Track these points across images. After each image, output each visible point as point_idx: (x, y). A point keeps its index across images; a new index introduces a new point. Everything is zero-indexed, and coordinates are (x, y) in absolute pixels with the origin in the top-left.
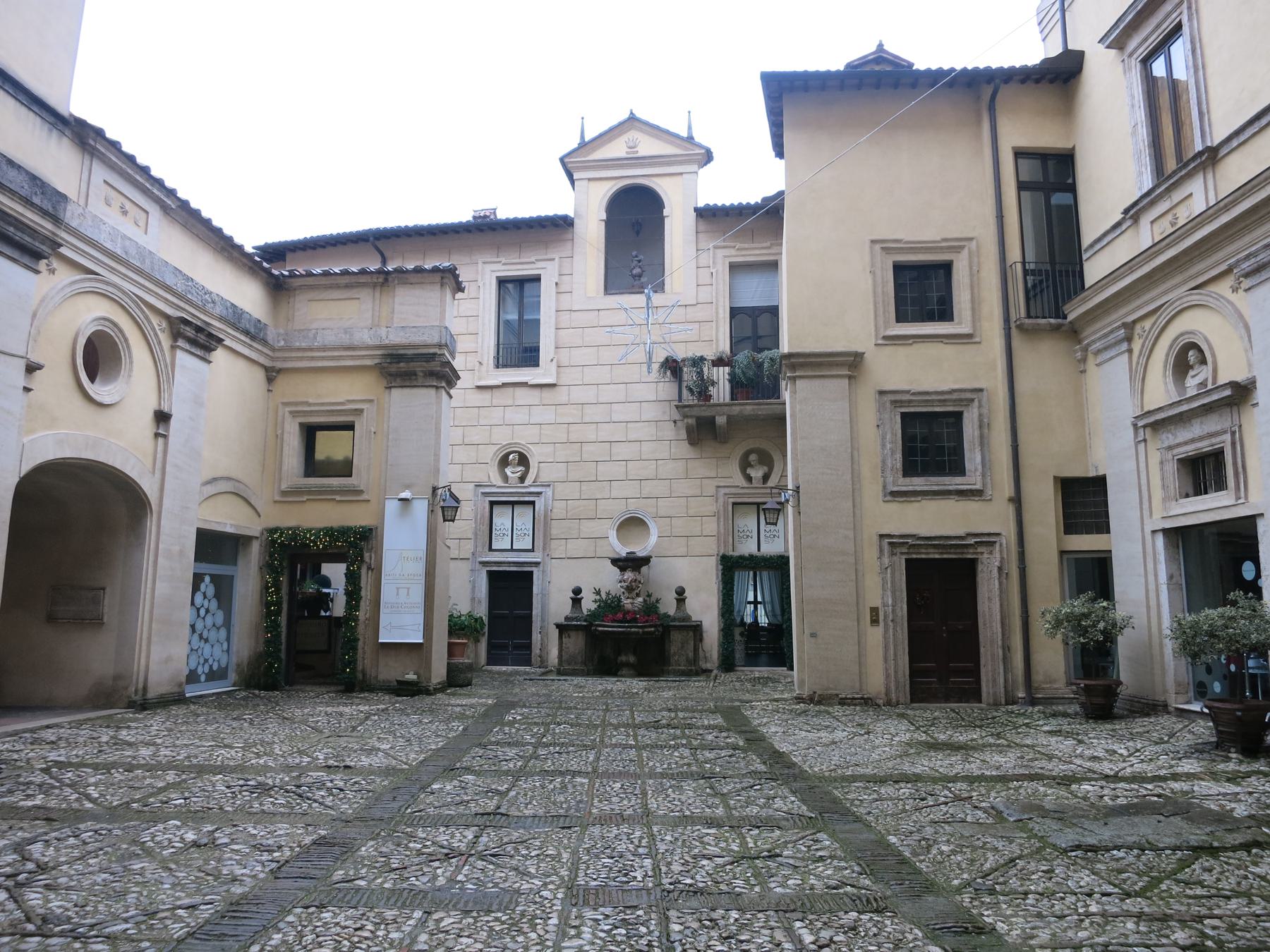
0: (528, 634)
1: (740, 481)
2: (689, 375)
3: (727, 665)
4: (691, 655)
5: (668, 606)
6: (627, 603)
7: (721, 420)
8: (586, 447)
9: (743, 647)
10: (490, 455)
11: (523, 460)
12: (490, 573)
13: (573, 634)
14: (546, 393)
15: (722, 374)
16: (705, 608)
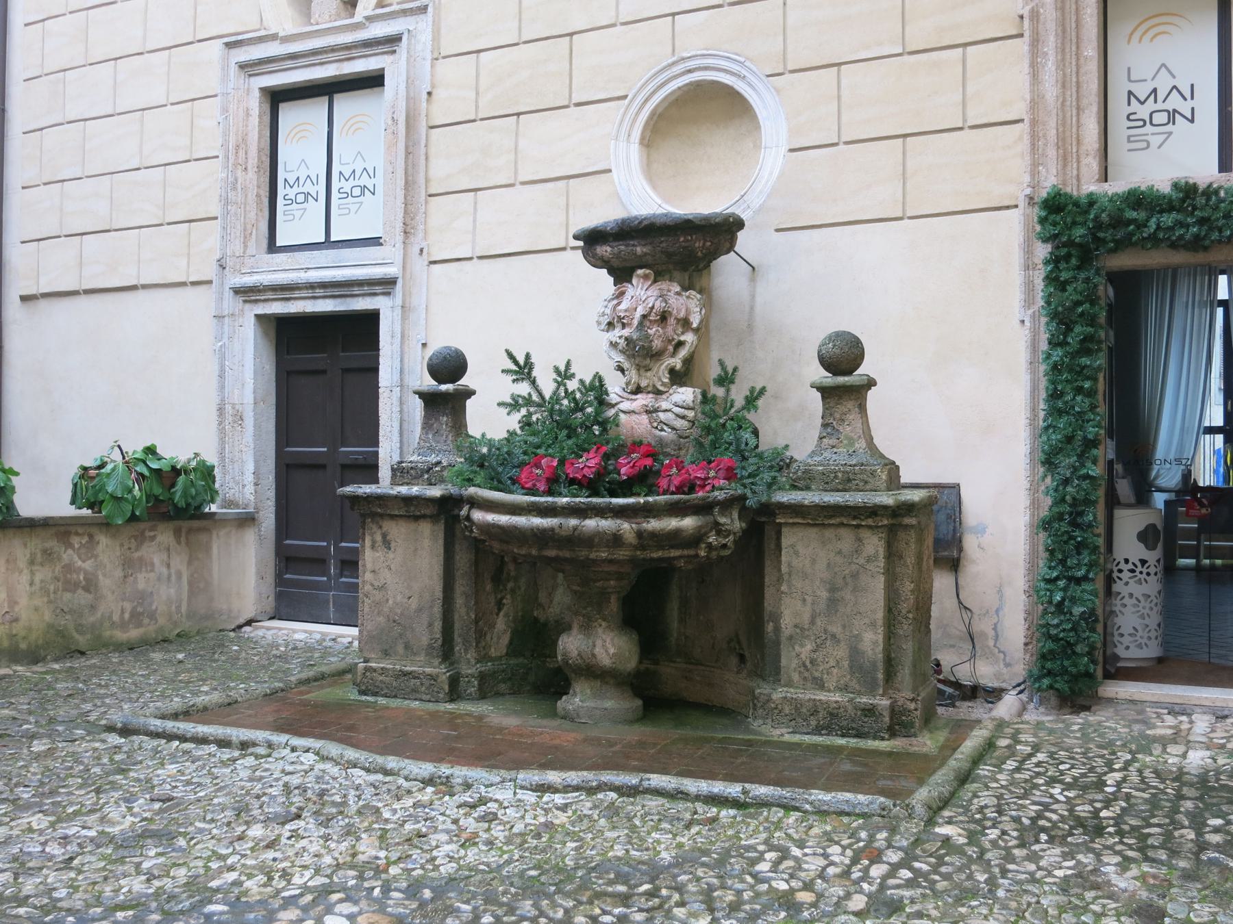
4: (872, 641)
5: (792, 424)
9: (1153, 586)
13: (398, 531)
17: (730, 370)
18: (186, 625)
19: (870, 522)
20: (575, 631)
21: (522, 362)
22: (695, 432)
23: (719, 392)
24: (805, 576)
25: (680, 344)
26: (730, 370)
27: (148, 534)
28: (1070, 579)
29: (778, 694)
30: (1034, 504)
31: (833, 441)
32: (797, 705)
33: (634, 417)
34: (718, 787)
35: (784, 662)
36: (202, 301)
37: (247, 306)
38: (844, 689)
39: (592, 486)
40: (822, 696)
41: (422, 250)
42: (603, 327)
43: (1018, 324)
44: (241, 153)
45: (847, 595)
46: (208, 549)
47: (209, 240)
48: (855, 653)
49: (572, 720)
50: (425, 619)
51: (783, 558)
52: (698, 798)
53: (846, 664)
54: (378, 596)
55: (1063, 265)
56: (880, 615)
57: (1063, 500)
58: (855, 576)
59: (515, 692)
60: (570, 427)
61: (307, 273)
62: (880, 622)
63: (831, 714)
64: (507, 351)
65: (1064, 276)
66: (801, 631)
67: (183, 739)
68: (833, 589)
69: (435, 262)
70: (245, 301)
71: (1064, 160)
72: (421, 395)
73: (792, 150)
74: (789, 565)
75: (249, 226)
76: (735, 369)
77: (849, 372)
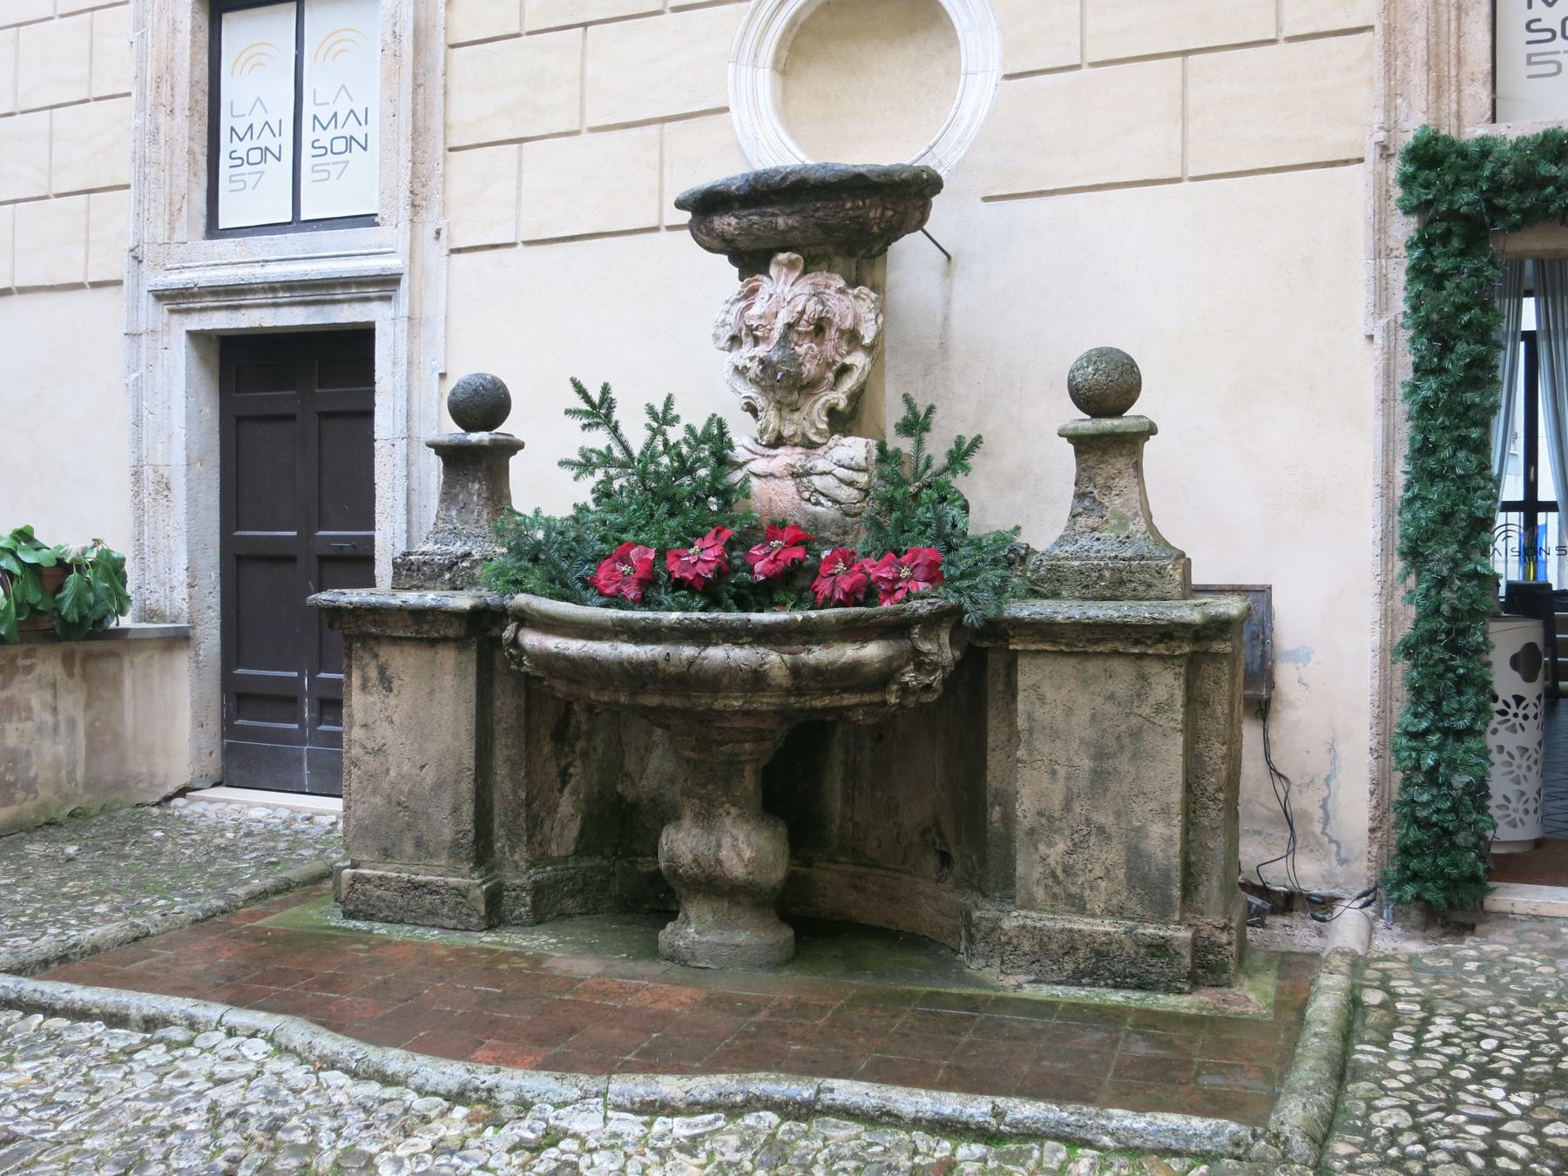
4: (1162, 838)
5: (1024, 492)
9: (1530, 735)
13: (404, 662)
17: (922, 411)
18: (84, 799)
19: (1161, 649)
20: (687, 822)
21: (596, 398)
22: (870, 508)
23: (906, 445)
24: (1055, 735)
25: (845, 370)
26: (922, 411)
27: (21, 662)
28: (1446, 732)
29: (1012, 921)
30: (1388, 618)
31: (1093, 521)
32: (1042, 938)
33: (773, 483)
34: (950, 1104)
35: (1020, 869)
36: (107, 312)
37: (176, 318)
38: (1117, 913)
39: (710, 591)
40: (1082, 924)
41: (438, 232)
42: (724, 343)
43: (1363, 342)
44: (165, 88)
45: (1123, 764)
46: (117, 684)
47: (117, 220)
48: (1135, 856)
49: (684, 963)
50: (447, 799)
51: (1021, 706)
52: (916, 1123)
53: (1121, 873)
54: (372, 764)
55: (1437, 249)
56: (1176, 796)
57: (1437, 611)
58: (1136, 734)
59: (590, 911)
60: (673, 504)
61: (266, 268)
62: (1176, 808)
63: (1098, 953)
64: (573, 380)
65: (1441, 265)
66: (1048, 823)
67: (50, 1011)
68: (1100, 755)
69: (459, 251)
70: (172, 311)
71: (1439, 88)
72: (441, 449)
73: (1008, 77)
74: (1030, 717)
75: (177, 198)
76: (931, 410)
77: (1118, 412)
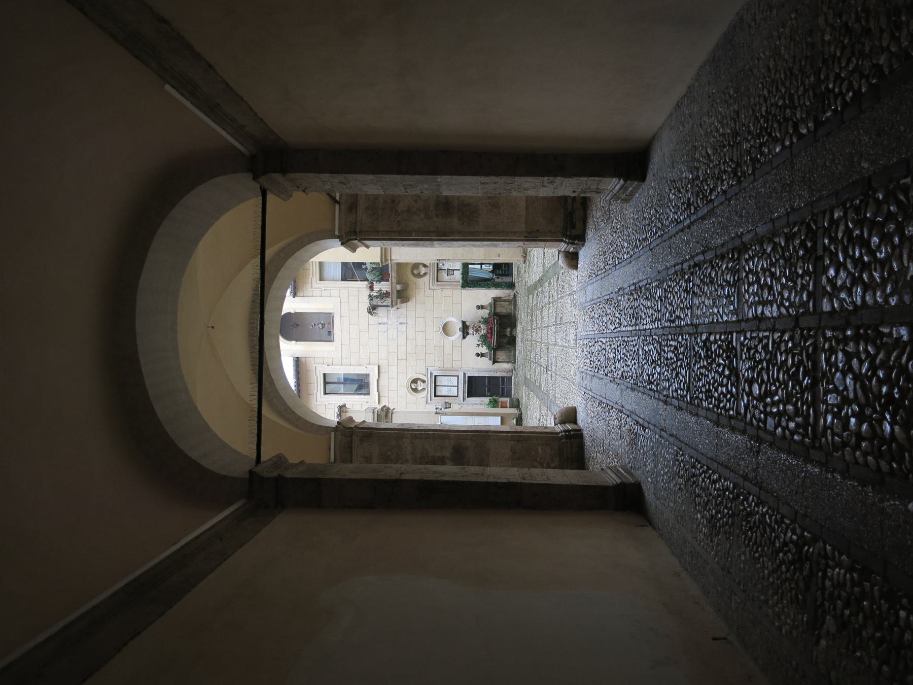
0: (497, 378)
1: (426, 278)
2: (376, 302)
3: (511, 286)
5: (485, 313)
6: (483, 332)
7: (399, 287)
8: (409, 351)
10: (412, 397)
11: (415, 381)
12: (469, 396)
14: (382, 370)
15: (377, 286)
16: (485, 296)
61: (463, 388)
